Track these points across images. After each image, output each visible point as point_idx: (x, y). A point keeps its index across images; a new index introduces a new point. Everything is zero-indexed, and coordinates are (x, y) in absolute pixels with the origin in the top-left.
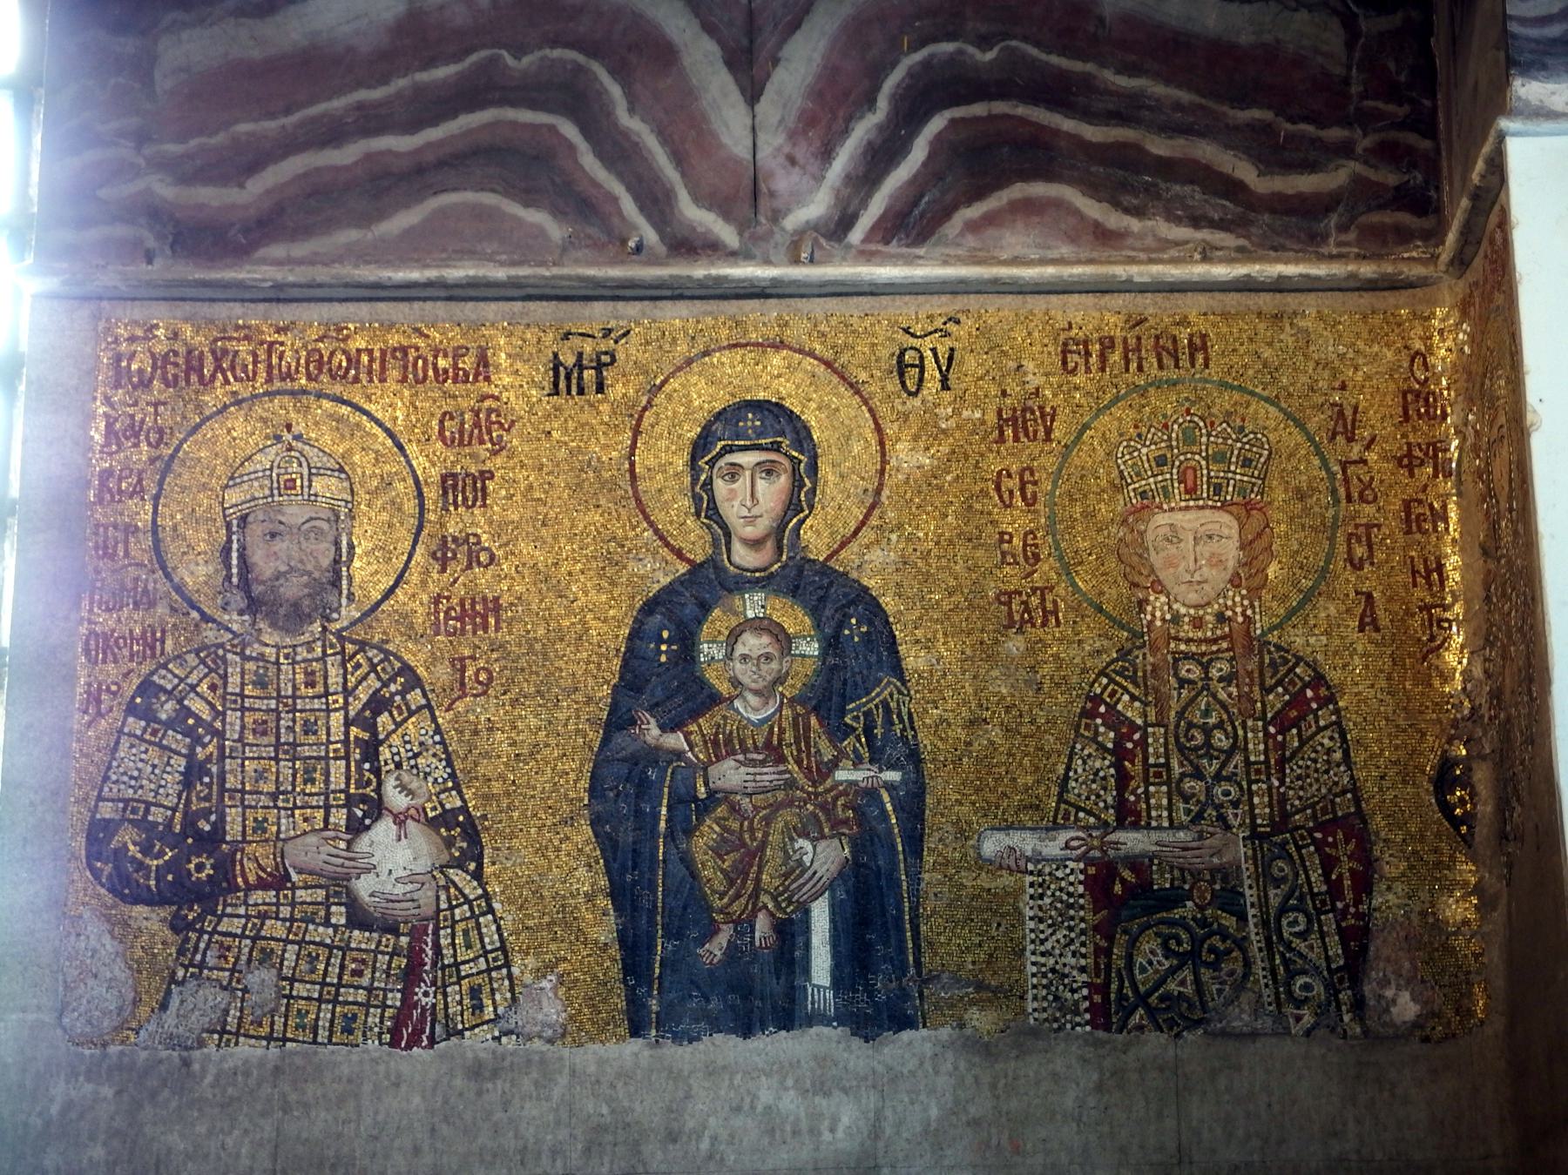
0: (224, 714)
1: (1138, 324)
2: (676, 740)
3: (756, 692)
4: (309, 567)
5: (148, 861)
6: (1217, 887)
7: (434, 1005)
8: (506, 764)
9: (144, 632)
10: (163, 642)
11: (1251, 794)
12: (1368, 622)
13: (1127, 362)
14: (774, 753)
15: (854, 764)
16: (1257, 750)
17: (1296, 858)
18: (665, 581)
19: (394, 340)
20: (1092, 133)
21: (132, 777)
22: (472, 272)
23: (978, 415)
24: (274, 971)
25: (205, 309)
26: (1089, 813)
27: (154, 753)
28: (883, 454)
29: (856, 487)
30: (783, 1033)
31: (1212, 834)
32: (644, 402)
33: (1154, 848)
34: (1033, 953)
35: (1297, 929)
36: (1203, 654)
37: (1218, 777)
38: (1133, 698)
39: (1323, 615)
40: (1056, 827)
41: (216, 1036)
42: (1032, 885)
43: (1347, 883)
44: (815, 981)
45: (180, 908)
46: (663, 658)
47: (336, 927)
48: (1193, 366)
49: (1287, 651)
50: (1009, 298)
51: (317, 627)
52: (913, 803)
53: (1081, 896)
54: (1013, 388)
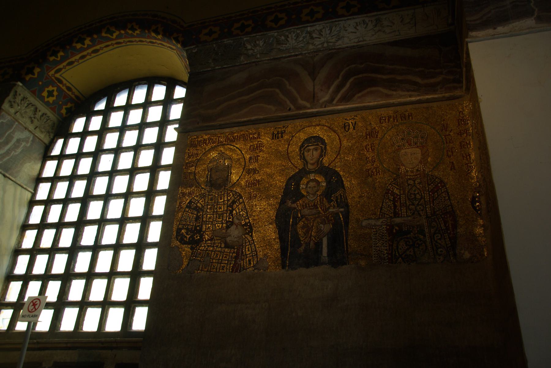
0: (204, 206)
1: (396, 112)
2: (294, 205)
3: (312, 194)
4: (223, 177)
5: (187, 236)
6: (418, 229)
7: (241, 264)
8: (258, 213)
9: (190, 191)
10: (194, 193)
11: (426, 208)
12: (453, 168)
13: (394, 120)
14: (315, 206)
15: (333, 208)
16: (427, 198)
17: (437, 221)
18: (293, 173)
19: (242, 133)
20: (384, 77)
21: (186, 220)
22: (256, 117)
23: (361, 134)
24: (209, 257)
25: (208, 132)
26: (387, 215)
27: (190, 214)
28: (341, 144)
29: (334, 151)
30: (316, 267)
31: (417, 217)
32: (291, 139)
33: (404, 221)
34: (374, 247)
35: (438, 238)
36: (413, 178)
37: (418, 205)
38: (397, 189)
39: (442, 168)
40: (379, 218)
41: (197, 271)
42: (374, 231)
43: (450, 226)
44: (323, 255)
45: (192, 245)
46: (292, 189)
47: (222, 248)
48: (409, 119)
49: (434, 176)
50: (368, 111)
51: (223, 188)
52: (347, 215)
53: (385, 233)
54: (369, 128)
